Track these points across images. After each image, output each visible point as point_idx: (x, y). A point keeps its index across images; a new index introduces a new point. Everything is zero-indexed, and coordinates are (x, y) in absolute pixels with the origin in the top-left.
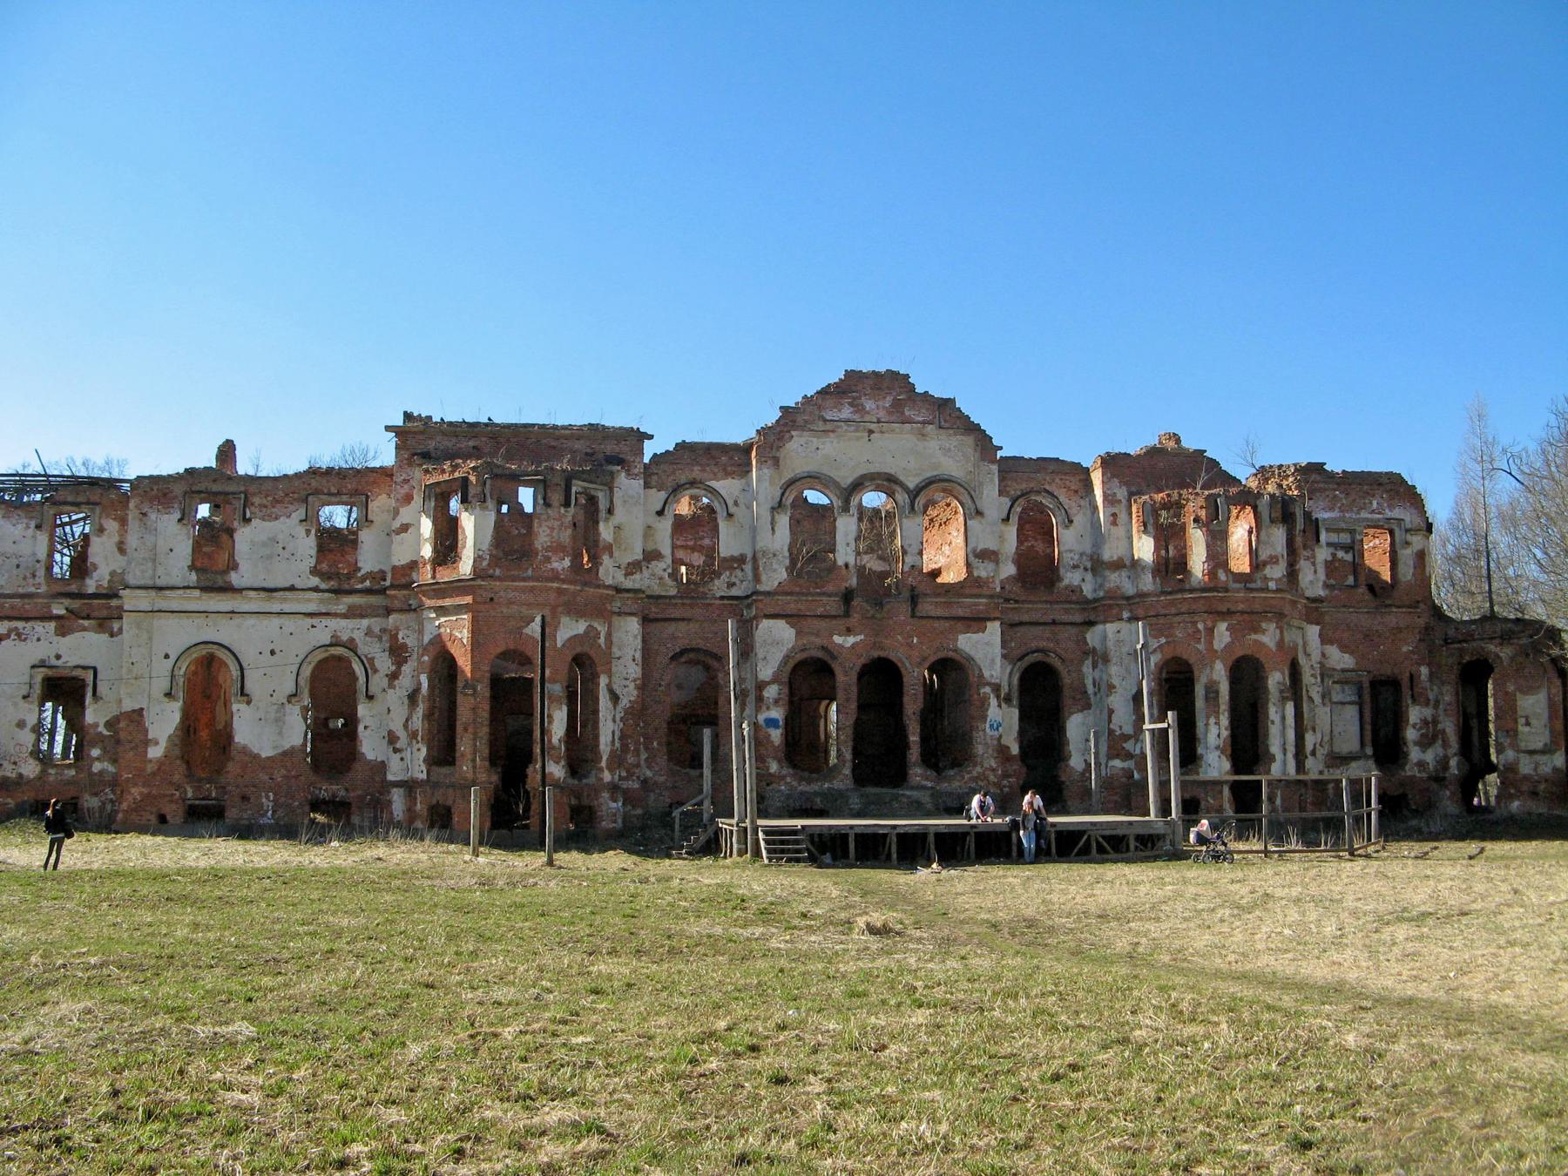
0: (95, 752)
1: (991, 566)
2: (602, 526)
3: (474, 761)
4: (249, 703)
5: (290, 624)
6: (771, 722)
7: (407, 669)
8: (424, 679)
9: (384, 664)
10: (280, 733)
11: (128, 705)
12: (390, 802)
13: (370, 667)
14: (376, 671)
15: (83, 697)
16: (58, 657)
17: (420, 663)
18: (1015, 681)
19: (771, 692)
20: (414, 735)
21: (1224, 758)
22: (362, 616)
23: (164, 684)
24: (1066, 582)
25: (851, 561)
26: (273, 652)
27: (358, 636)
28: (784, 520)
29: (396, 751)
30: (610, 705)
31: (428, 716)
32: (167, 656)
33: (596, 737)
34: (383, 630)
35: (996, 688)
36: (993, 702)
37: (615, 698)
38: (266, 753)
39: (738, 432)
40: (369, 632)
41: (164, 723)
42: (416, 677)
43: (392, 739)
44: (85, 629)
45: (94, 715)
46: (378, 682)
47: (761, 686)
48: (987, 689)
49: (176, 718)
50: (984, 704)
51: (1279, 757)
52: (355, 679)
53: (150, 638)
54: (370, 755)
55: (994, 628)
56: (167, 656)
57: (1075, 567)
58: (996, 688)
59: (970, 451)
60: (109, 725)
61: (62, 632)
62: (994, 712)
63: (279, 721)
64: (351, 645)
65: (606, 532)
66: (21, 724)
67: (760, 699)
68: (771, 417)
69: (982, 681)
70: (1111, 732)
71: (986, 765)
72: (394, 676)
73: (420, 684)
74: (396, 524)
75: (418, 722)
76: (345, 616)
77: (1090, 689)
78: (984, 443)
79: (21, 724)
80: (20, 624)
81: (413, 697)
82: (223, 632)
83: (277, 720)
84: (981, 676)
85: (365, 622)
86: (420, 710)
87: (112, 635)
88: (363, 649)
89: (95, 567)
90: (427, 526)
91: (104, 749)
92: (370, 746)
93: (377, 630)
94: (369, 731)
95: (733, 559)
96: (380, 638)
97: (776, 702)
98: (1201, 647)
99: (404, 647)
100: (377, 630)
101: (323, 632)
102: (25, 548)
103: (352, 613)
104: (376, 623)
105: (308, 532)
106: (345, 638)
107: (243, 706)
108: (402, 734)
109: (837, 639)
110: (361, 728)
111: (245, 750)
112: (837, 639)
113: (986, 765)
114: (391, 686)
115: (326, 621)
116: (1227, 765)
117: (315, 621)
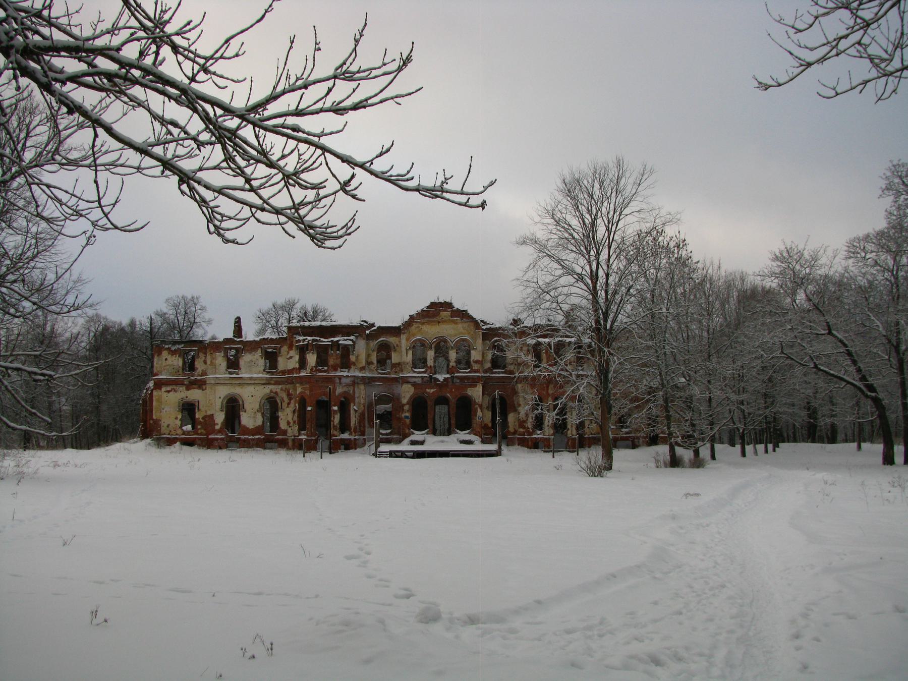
0: (199, 427)
1: (479, 366)
2: (351, 356)
3: (311, 430)
4: (245, 412)
5: (257, 388)
6: (407, 417)
7: (292, 401)
8: (297, 405)
9: (286, 400)
10: (255, 421)
11: (209, 413)
12: (288, 443)
13: (282, 400)
14: (284, 401)
15: (195, 409)
16: (187, 397)
17: (296, 400)
18: (490, 402)
19: (406, 408)
20: (294, 422)
21: (550, 429)
22: (279, 384)
23: (220, 407)
24: (508, 369)
25: (432, 365)
26: (252, 396)
27: (278, 390)
28: (410, 352)
29: (290, 427)
30: (354, 412)
31: (299, 417)
32: (220, 398)
33: (350, 422)
34: (286, 389)
35: (481, 406)
36: (479, 410)
37: (356, 411)
38: (251, 427)
39: (396, 323)
40: (282, 389)
41: (220, 418)
42: (295, 404)
43: (288, 423)
44: (194, 388)
45: (198, 415)
46: (285, 405)
47: (404, 405)
48: (477, 406)
49: (224, 416)
50: (476, 411)
51: (570, 429)
52: (278, 404)
53: (215, 392)
54: (283, 428)
55: (479, 388)
56: (220, 398)
57: (512, 364)
58: (481, 406)
59: (472, 327)
60: (203, 418)
61: (188, 389)
62: (479, 413)
63: (255, 417)
64: (276, 393)
65: (353, 358)
66: (176, 418)
67: (403, 409)
68: (407, 318)
69: (475, 403)
70: (519, 420)
71: (476, 430)
72: (289, 404)
73: (296, 406)
74: (288, 357)
75: (296, 418)
76: (274, 384)
77: (516, 405)
78: (476, 324)
79: (176, 418)
80: (175, 387)
81: (294, 412)
82: (237, 390)
83: (254, 417)
84: (475, 401)
85: (280, 386)
86: (296, 415)
87: (203, 390)
88: (280, 395)
89: (197, 368)
90: (297, 358)
91: (202, 426)
92: (283, 425)
93: (284, 389)
94: (282, 421)
95: (396, 364)
96: (285, 391)
97: (408, 411)
98: (545, 393)
99: (292, 395)
100: (284, 389)
101: (267, 390)
102: (175, 363)
103: (277, 383)
104: (284, 386)
105: (262, 358)
106: (274, 391)
107: (243, 413)
108: (291, 422)
109: (428, 390)
110: (280, 419)
111: (244, 426)
112: (428, 390)
113: (476, 430)
114: (288, 407)
115: (268, 386)
116: (552, 432)
117: (265, 386)
